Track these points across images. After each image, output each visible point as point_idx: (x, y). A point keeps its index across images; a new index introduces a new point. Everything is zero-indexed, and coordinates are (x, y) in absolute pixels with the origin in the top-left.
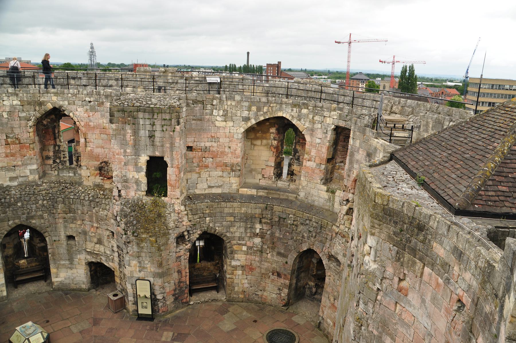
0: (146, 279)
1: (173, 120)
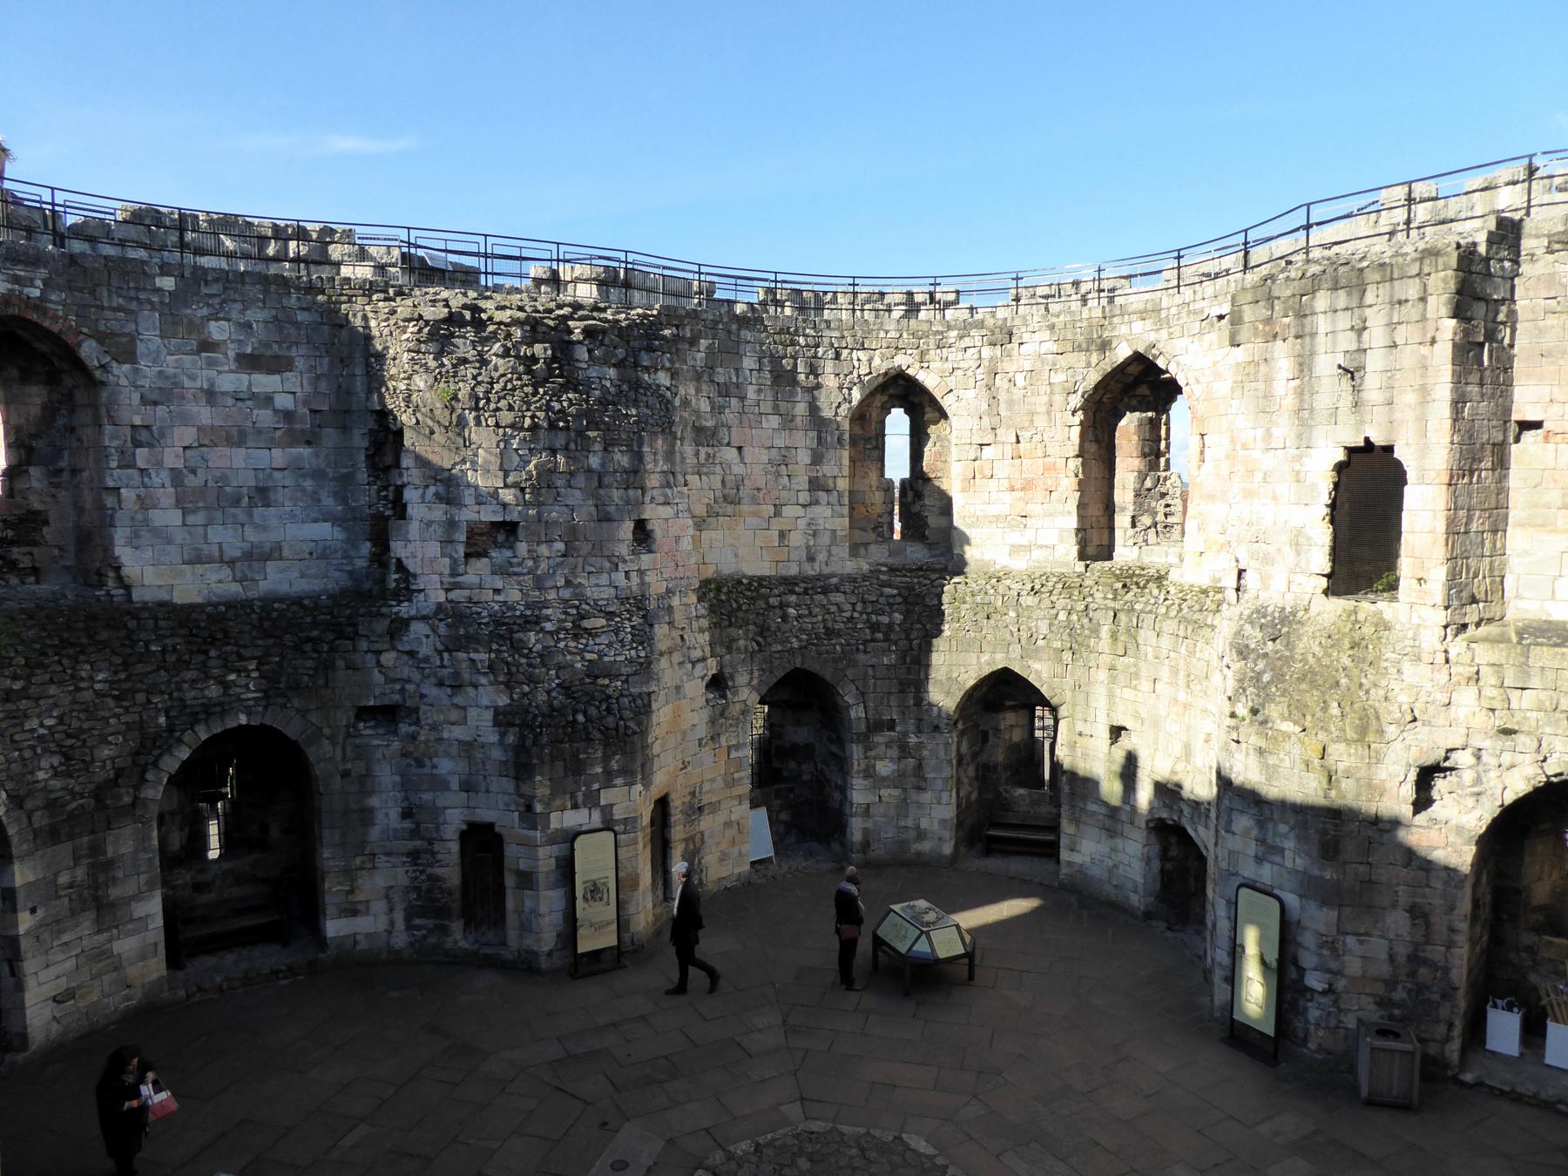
0: (1276, 892)
1: (1431, 300)
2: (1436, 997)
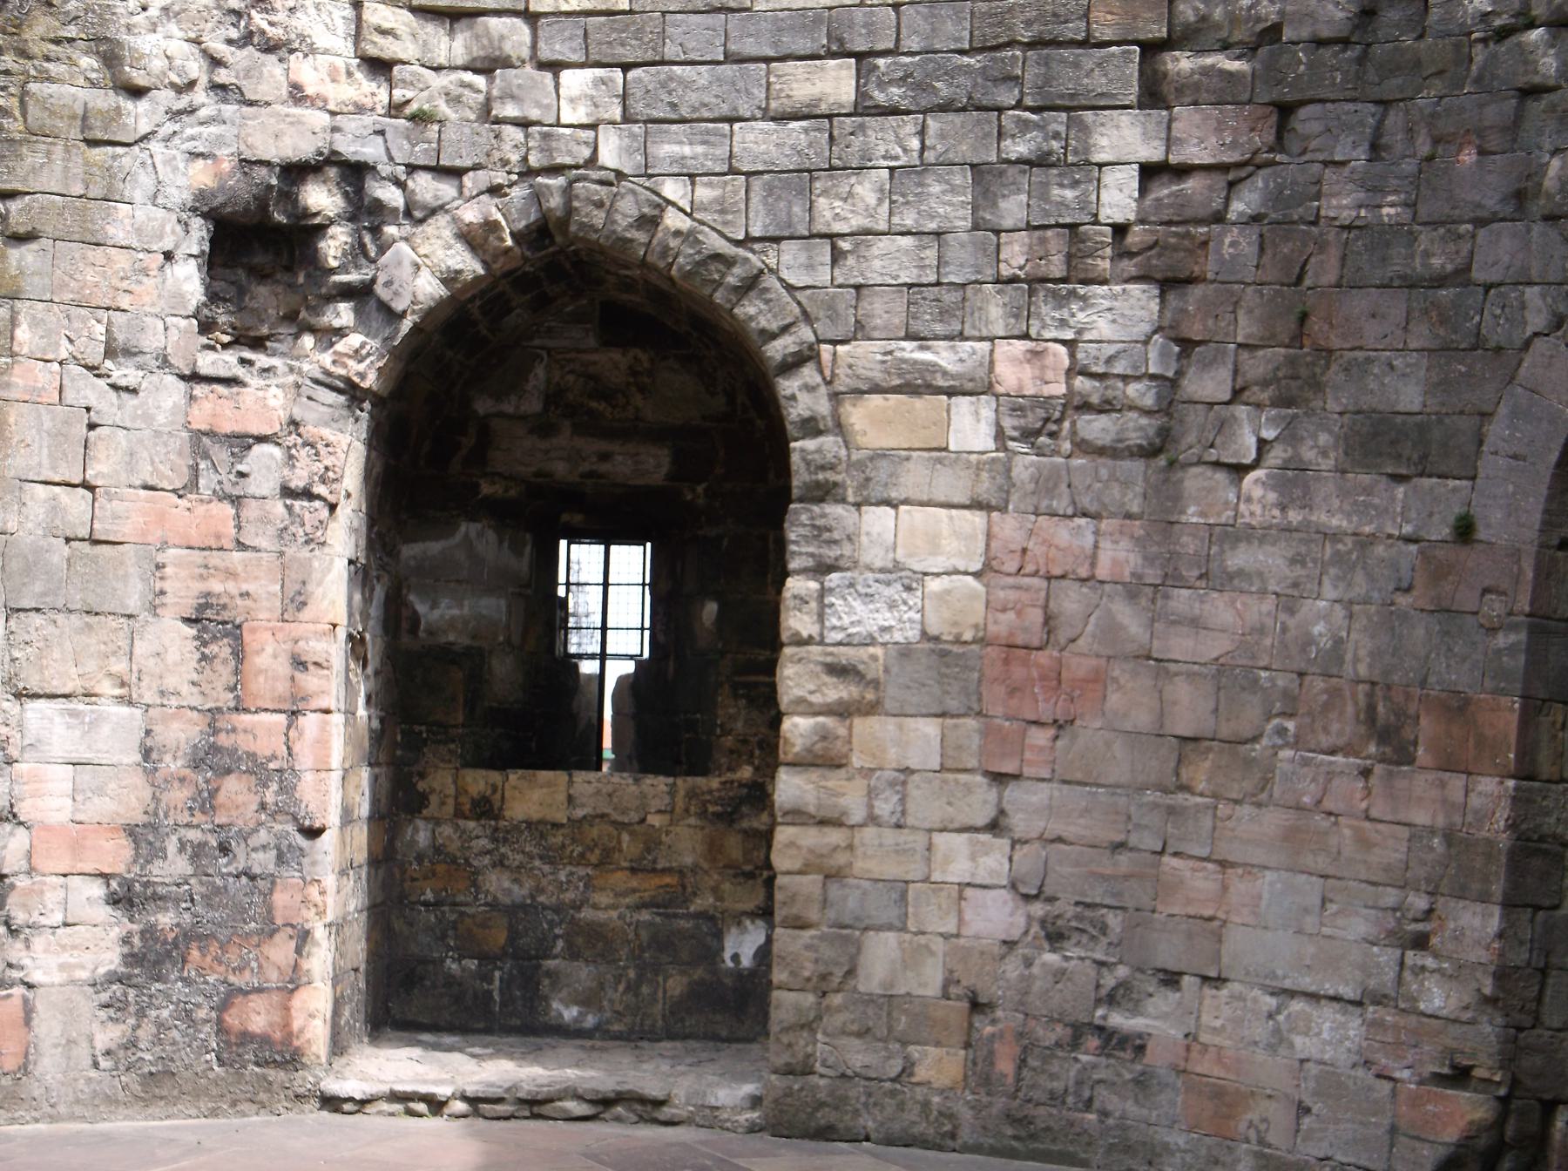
2: (263, 861)
